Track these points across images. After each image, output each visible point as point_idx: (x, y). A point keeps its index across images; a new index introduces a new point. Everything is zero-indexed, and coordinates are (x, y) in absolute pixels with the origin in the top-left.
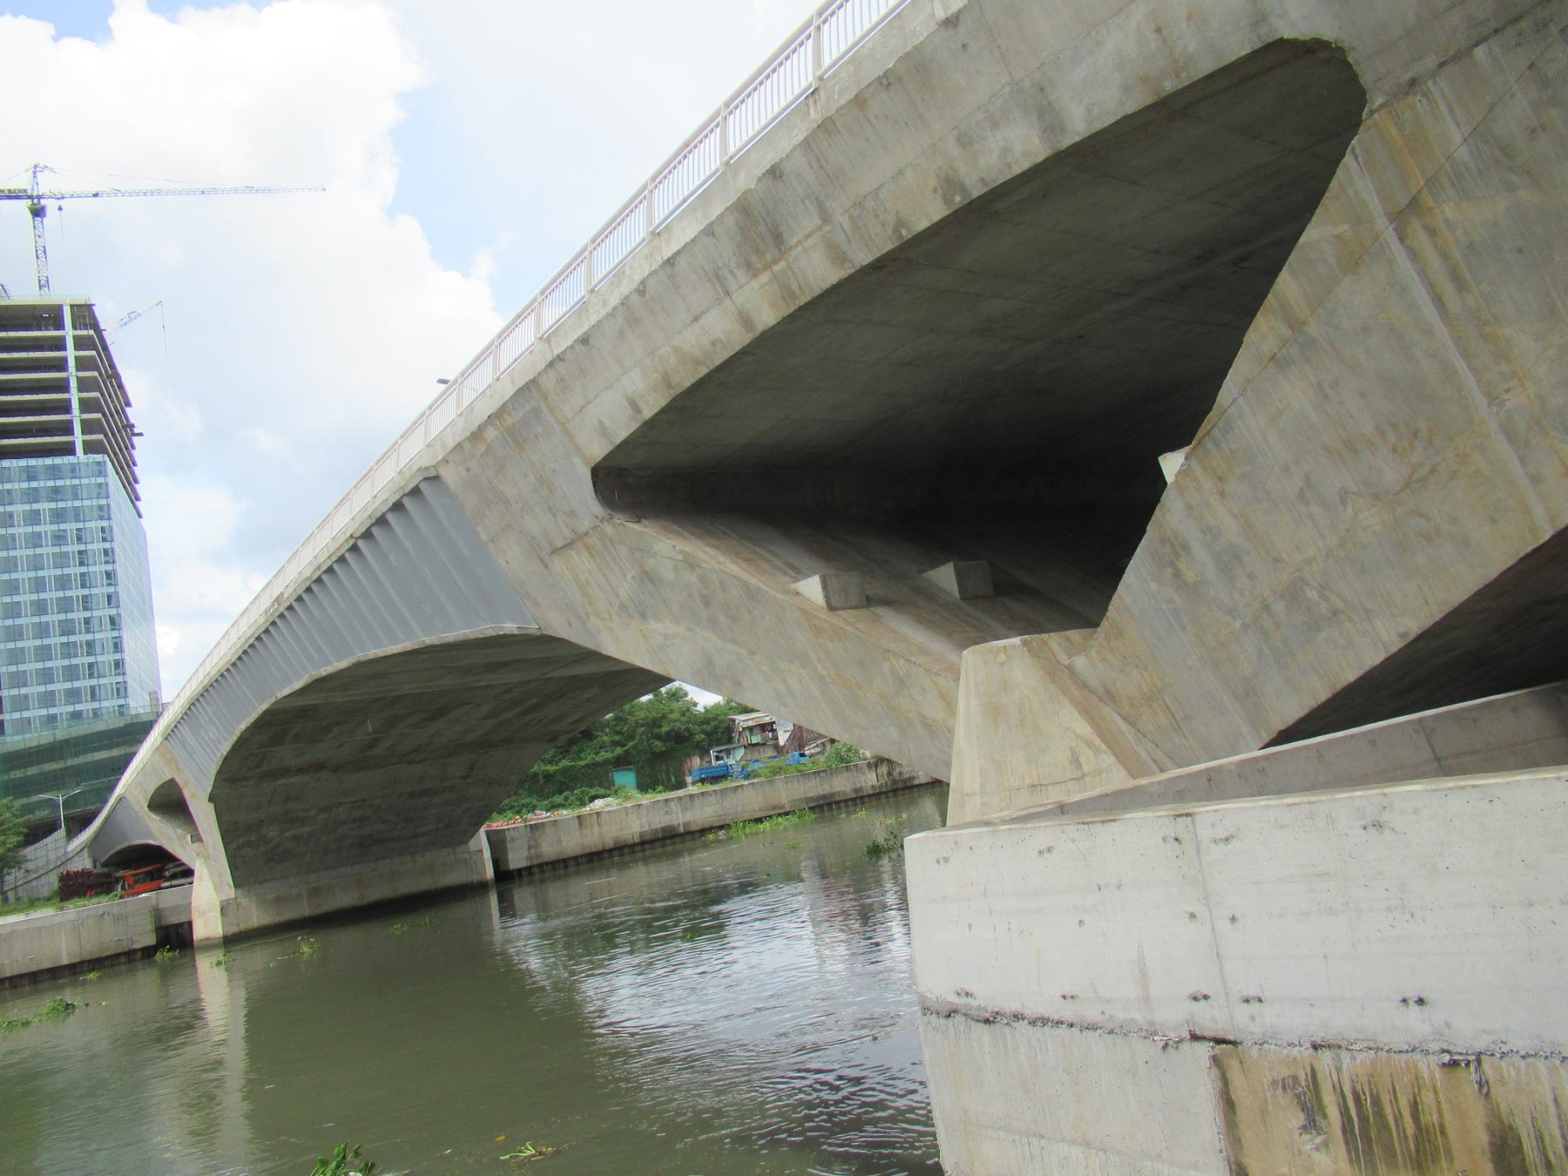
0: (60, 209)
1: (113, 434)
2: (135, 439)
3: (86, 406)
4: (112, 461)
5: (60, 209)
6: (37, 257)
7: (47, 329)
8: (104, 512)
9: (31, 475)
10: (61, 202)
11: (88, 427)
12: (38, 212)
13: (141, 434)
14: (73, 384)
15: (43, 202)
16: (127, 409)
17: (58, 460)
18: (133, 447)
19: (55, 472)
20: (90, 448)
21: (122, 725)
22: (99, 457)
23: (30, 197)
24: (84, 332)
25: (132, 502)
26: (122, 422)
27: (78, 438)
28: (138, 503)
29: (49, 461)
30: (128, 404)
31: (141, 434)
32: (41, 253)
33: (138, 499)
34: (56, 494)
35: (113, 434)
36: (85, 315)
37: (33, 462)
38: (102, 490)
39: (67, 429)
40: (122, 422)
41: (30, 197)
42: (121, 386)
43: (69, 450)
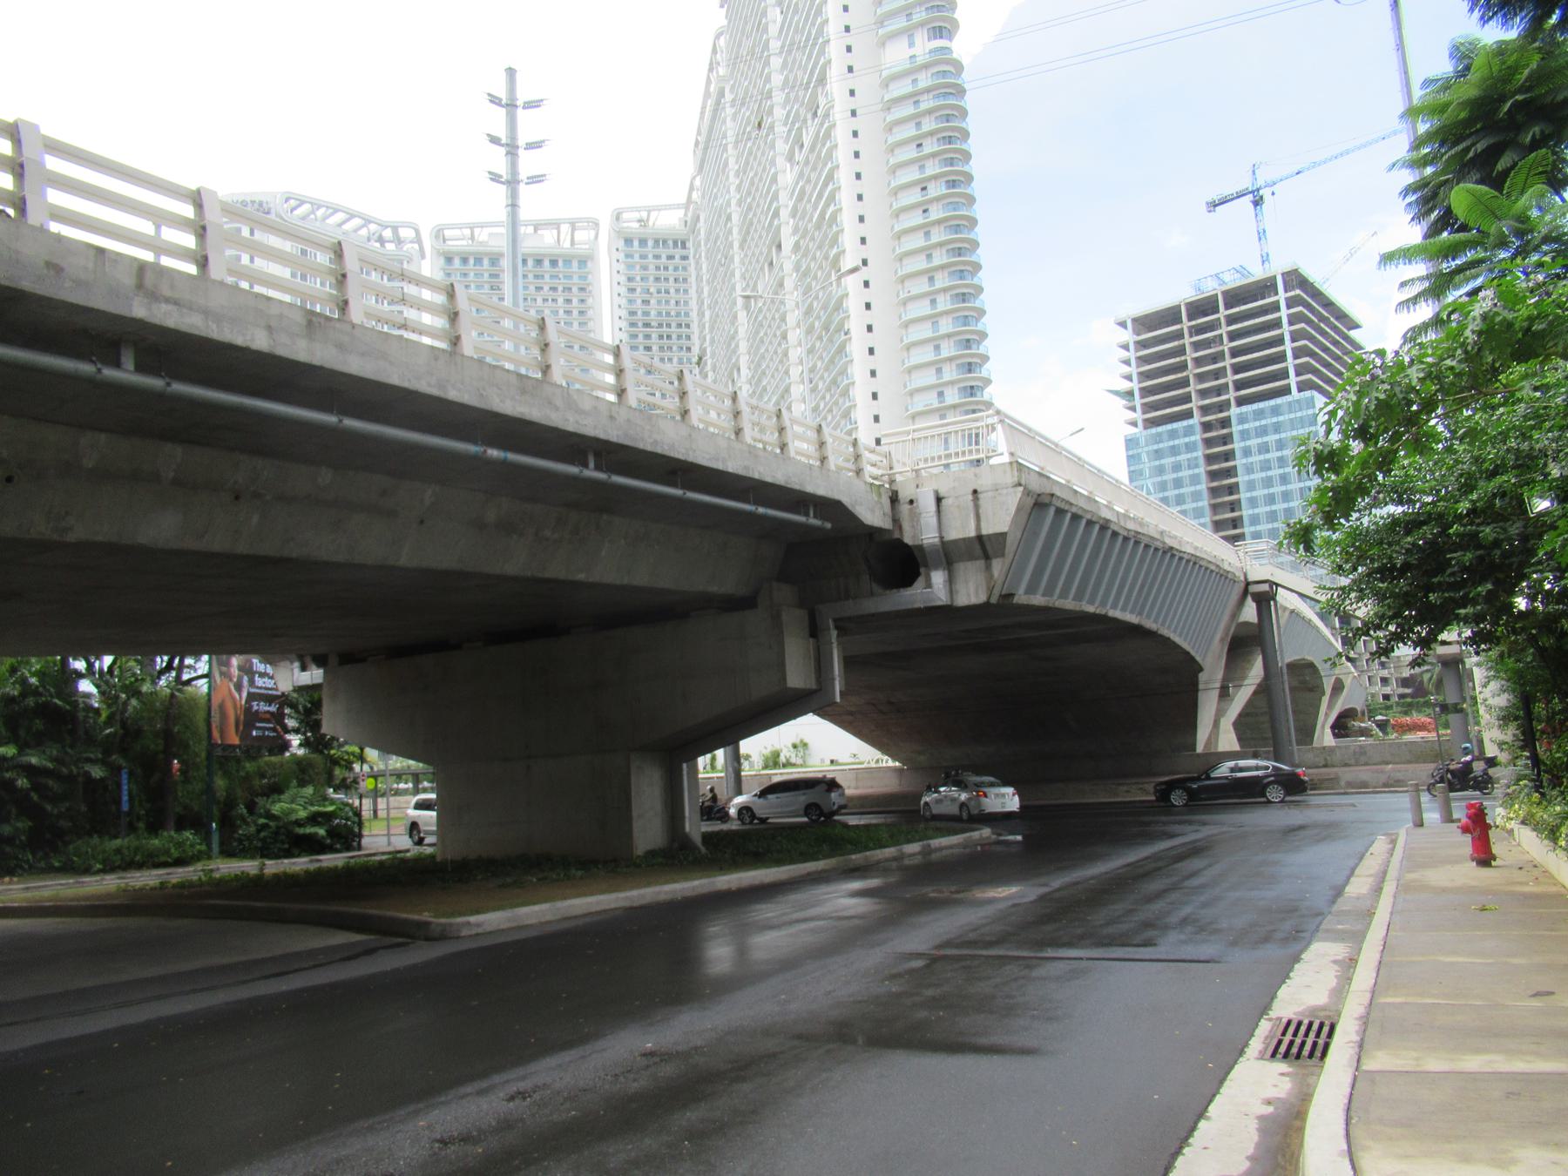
0: (1273, 194)
1: (1327, 365)
5: (1273, 194)
6: (1260, 239)
7: (1270, 296)
9: (1259, 414)
10: (1272, 189)
12: (1257, 202)
15: (1261, 192)
16: (1353, 334)
17: (1279, 401)
19: (1276, 411)
22: (1308, 394)
23: (1250, 193)
27: (1293, 380)
30: (1357, 326)
32: (1261, 235)
34: (1277, 428)
35: (1327, 365)
36: (1295, 279)
37: (1261, 405)
39: (1284, 374)
41: (1250, 193)
42: (1342, 316)
43: (1286, 391)
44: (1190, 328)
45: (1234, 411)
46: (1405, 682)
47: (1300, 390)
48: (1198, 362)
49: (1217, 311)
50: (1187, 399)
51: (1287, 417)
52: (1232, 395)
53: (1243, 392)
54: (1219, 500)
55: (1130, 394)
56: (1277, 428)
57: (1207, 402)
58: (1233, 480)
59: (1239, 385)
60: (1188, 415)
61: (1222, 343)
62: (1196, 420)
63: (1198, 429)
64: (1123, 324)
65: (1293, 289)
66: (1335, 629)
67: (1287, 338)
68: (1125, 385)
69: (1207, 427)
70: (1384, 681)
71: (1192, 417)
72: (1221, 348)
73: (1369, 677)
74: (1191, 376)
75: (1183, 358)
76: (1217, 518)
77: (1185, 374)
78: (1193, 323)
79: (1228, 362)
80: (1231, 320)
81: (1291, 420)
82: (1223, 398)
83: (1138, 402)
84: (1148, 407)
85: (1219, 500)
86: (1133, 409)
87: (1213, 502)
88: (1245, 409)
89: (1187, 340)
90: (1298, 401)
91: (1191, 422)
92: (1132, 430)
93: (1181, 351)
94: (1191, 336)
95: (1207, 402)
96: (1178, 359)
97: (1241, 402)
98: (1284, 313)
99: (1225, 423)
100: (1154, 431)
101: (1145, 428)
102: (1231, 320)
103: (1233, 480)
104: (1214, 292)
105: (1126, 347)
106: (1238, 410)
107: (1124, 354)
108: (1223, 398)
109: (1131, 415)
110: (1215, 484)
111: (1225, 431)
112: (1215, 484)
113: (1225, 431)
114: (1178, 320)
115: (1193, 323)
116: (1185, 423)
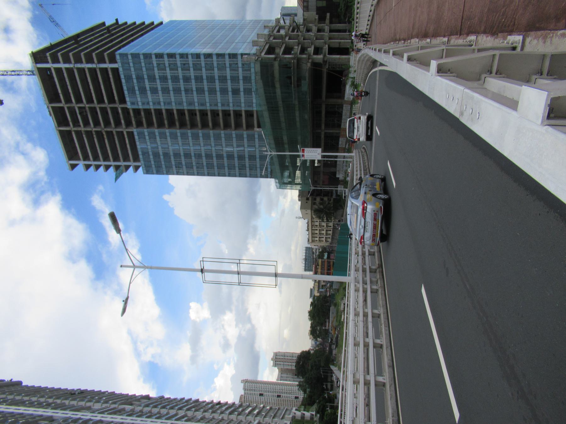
2: (120, 22)
3: (89, 60)
4: (120, 48)
8: (147, 56)
9: (132, 91)
11: (101, 60)
13: (117, 20)
14: (79, 66)
18: (126, 23)
19: (129, 78)
20: (113, 60)
21: (261, 81)
22: (118, 57)
24: (49, 58)
25: (152, 29)
26: (106, 33)
28: (156, 23)
29: (123, 81)
30: (104, 24)
31: (117, 20)
33: (152, 23)
34: (140, 78)
38: (135, 56)
39: (104, 71)
40: (106, 33)
43: (116, 71)
44: (74, 126)
45: (129, 106)
46: (322, 19)
47: (116, 62)
48: (97, 123)
49: (62, 108)
50: (121, 134)
51: (133, 73)
52: (119, 106)
53: (116, 98)
54: (188, 122)
55: (117, 168)
56: (140, 78)
57: (123, 122)
58: (175, 112)
59: (111, 100)
60: (131, 135)
61: (84, 108)
62: (135, 131)
63: (140, 130)
64: (73, 167)
65: (46, 57)
66: (275, 59)
67: (79, 66)
68: (112, 170)
69: (139, 124)
70: (319, 30)
71: (132, 133)
72: (87, 109)
73: (316, 39)
74: (105, 130)
75: (94, 133)
76: (199, 125)
77: (104, 133)
78: (71, 124)
79: (96, 105)
80: (68, 100)
81: (135, 70)
82: (120, 111)
83: (122, 163)
84: (126, 159)
85: (188, 122)
86: (127, 168)
87: (189, 126)
88: (128, 99)
89: (82, 128)
90: (122, 63)
91: (135, 133)
92: (141, 169)
93: (89, 134)
94: (80, 126)
95: (123, 122)
96: (95, 136)
97: (123, 100)
98: (62, 65)
99: (137, 112)
100: (141, 157)
101: (139, 161)
102: (68, 100)
103: (175, 112)
104: (50, 108)
105: (88, 167)
106: (129, 103)
107: (92, 169)
108: (120, 111)
109: (131, 169)
110: (177, 124)
111: (143, 113)
112: (177, 124)
113: (143, 113)
114: (69, 132)
115: (71, 124)
116: (136, 137)
